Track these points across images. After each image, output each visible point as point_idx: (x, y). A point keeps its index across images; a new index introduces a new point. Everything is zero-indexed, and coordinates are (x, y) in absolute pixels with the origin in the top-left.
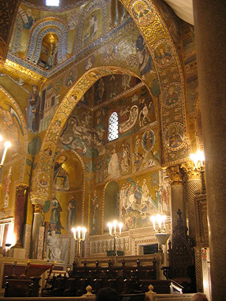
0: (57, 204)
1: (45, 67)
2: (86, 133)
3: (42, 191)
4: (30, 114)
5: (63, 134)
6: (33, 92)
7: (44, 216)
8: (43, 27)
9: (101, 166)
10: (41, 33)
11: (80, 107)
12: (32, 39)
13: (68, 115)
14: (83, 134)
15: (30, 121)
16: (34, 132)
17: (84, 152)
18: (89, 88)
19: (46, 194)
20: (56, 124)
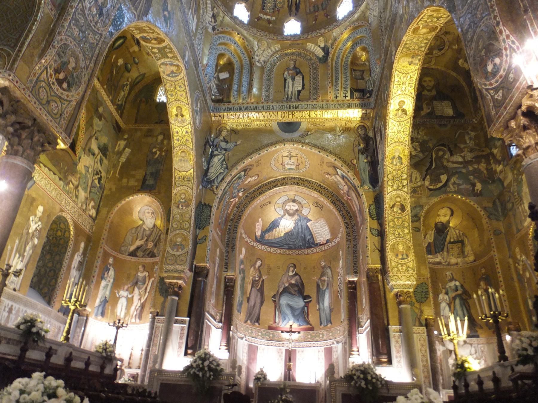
0: (459, 288)
1: (364, 96)
2: (474, 160)
3: (402, 269)
6: (360, 135)
7: (421, 309)
8: (344, 49)
9: (513, 203)
10: (345, 56)
11: (449, 126)
13: (407, 143)
14: (466, 163)
15: (363, 175)
16: (374, 187)
17: (477, 190)
19: (411, 272)
20: (395, 163)
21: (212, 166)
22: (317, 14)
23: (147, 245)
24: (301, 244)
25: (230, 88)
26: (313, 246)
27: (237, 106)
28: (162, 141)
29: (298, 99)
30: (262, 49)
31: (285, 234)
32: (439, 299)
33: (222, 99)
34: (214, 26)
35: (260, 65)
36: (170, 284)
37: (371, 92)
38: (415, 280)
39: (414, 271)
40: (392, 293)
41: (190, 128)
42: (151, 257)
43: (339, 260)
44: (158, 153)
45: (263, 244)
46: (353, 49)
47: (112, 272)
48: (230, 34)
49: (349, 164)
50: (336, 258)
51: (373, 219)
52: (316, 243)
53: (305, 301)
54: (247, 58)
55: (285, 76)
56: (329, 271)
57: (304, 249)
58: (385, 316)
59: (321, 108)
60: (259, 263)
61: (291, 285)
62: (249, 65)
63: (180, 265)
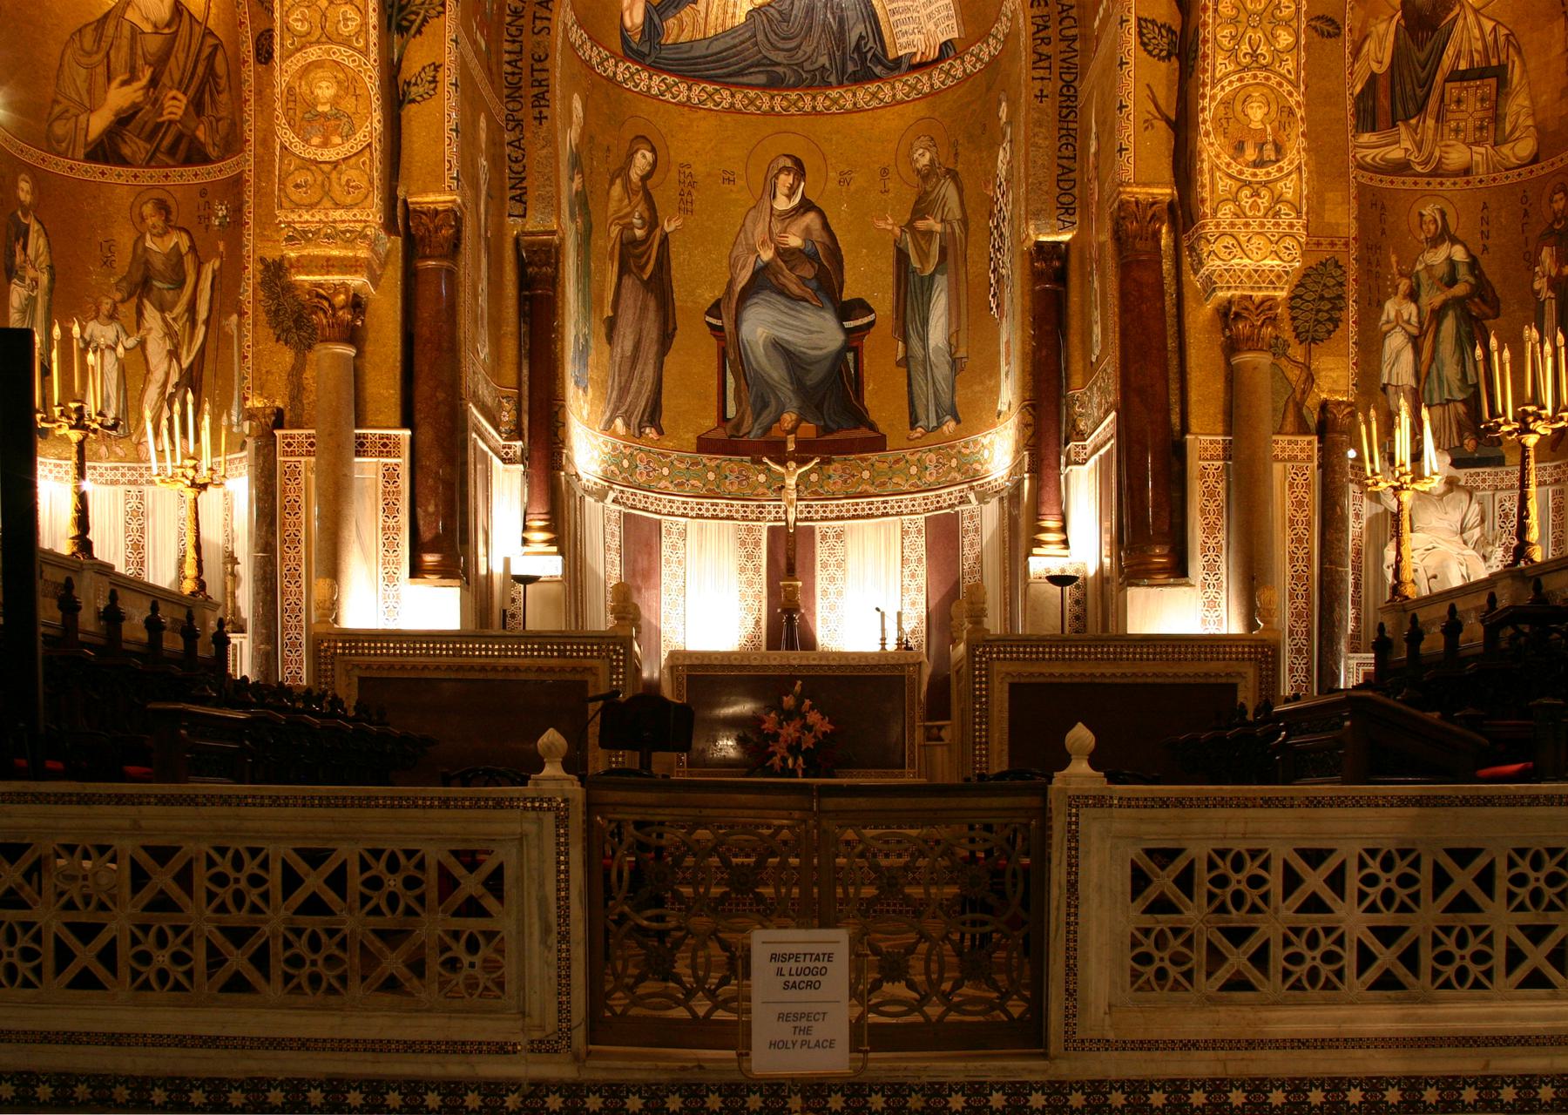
3: (1254, 206)
24: (824, 60)
26: (878, 70)
31: (750, 14)
36: (316, 292)
38: (1297, 252)
39: (1299, 213)
40: (1209, 307)
43: (994, 145)
45: (657, 68)
50: (986, 136)
52: (891, 55)
56: (949, 191)
57: (840, 84)
60: (642, 160)
63: (348, 207)
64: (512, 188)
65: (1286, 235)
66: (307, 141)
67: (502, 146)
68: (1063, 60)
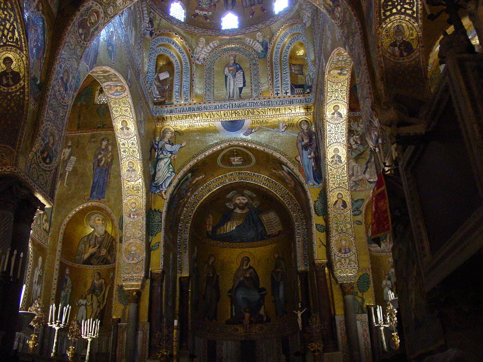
1: (304, 91)
4: (306, 161)
5: (367, 168)
6: (303, 130)
7: (362, 298)
8: (282, 44)
10: (284, 51)
12: (274, 66)
15: (308, 171)
16: (319, 183)
18: (348, 93)
21: (159, 170)
22: (253, 7)
23: (100, 252)
24: (253, 236)
25: (171, 90)
27: (180, 107)
28: (107, 147)
29: (240, 98)
30: (201, 46)
32: (383, 285)
33: (165, 101)
34: (152, 30)
35: (200, 63)
37: (310, 87)
39: (356, 263)
41: (136, 140)
42: (105, 264)
44: (104, 159)
46: (291, 44)
47: (69, 282)
48: (168, 35)
49: (293, 161)
51: (318, 215)
53: (261, 293)
54: (186, 57)
55: (225, 73)
58: (332, 307)
59: (262, 105)
60: (212, 260)
61: (246, 278)
62: (189, 64)
63: (137, 273)
64: (179, 267)
65: (353, 268)
66: (129, 259)
67: (177, 258)
68: (303, 233)
